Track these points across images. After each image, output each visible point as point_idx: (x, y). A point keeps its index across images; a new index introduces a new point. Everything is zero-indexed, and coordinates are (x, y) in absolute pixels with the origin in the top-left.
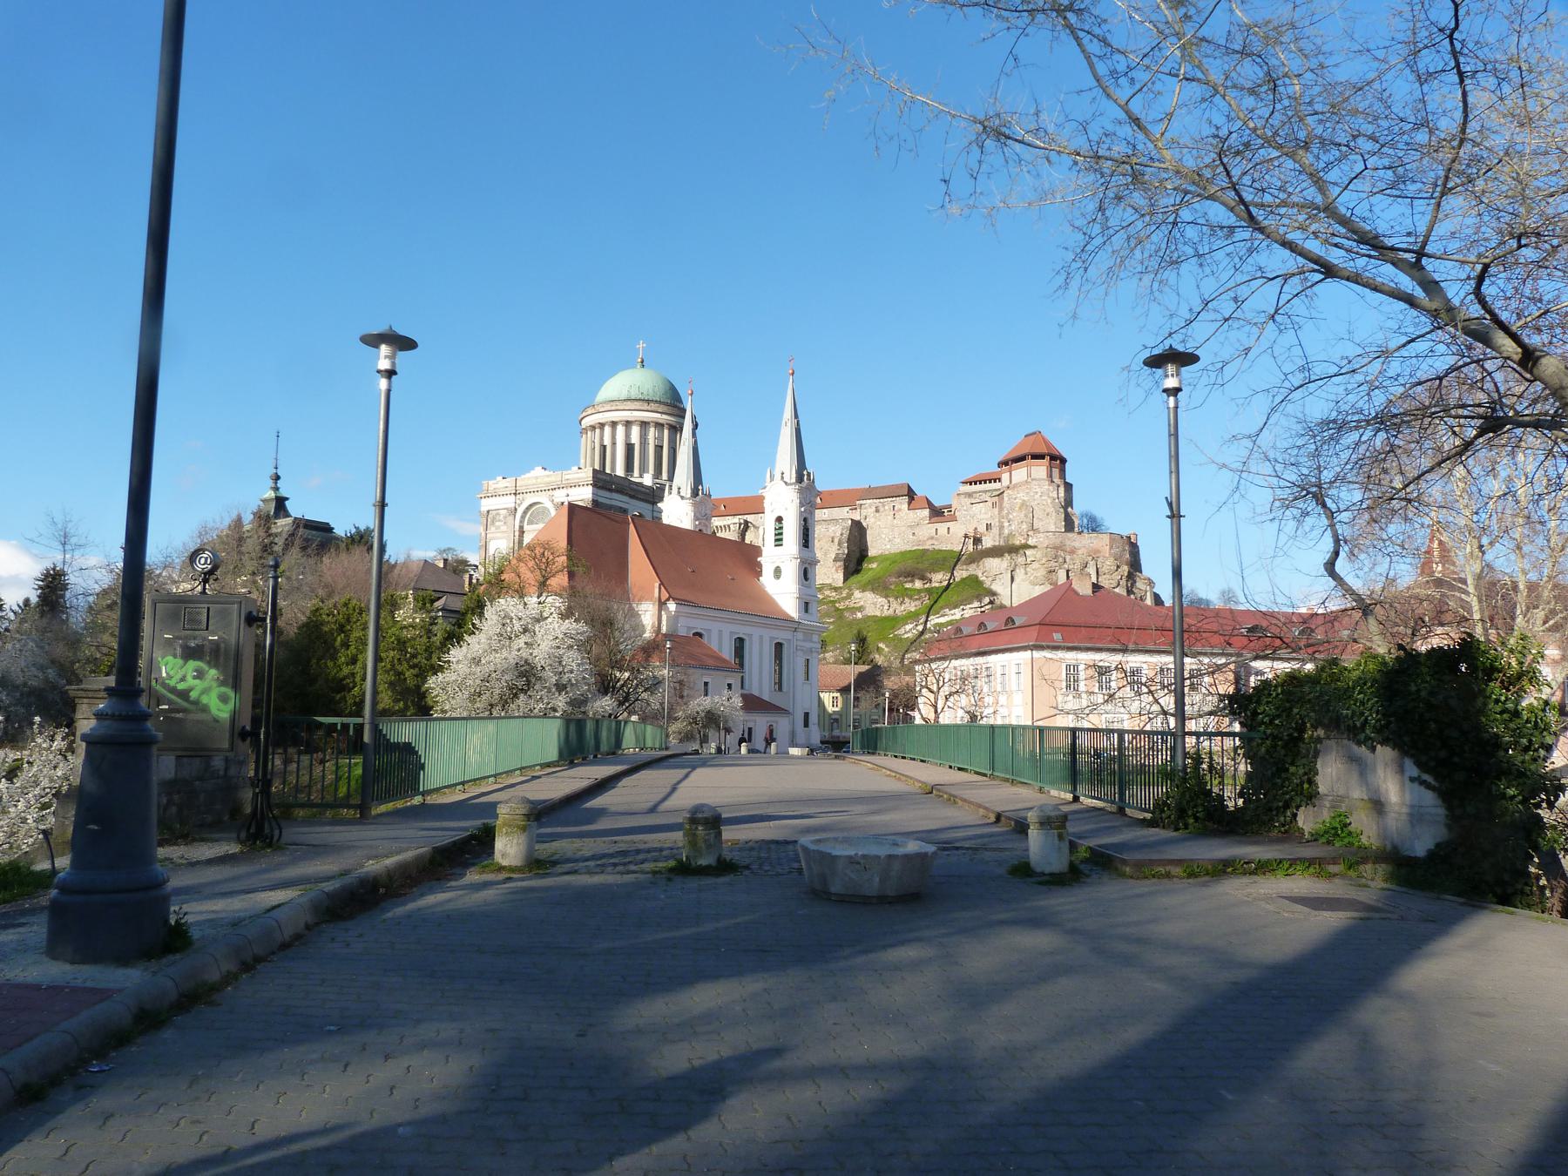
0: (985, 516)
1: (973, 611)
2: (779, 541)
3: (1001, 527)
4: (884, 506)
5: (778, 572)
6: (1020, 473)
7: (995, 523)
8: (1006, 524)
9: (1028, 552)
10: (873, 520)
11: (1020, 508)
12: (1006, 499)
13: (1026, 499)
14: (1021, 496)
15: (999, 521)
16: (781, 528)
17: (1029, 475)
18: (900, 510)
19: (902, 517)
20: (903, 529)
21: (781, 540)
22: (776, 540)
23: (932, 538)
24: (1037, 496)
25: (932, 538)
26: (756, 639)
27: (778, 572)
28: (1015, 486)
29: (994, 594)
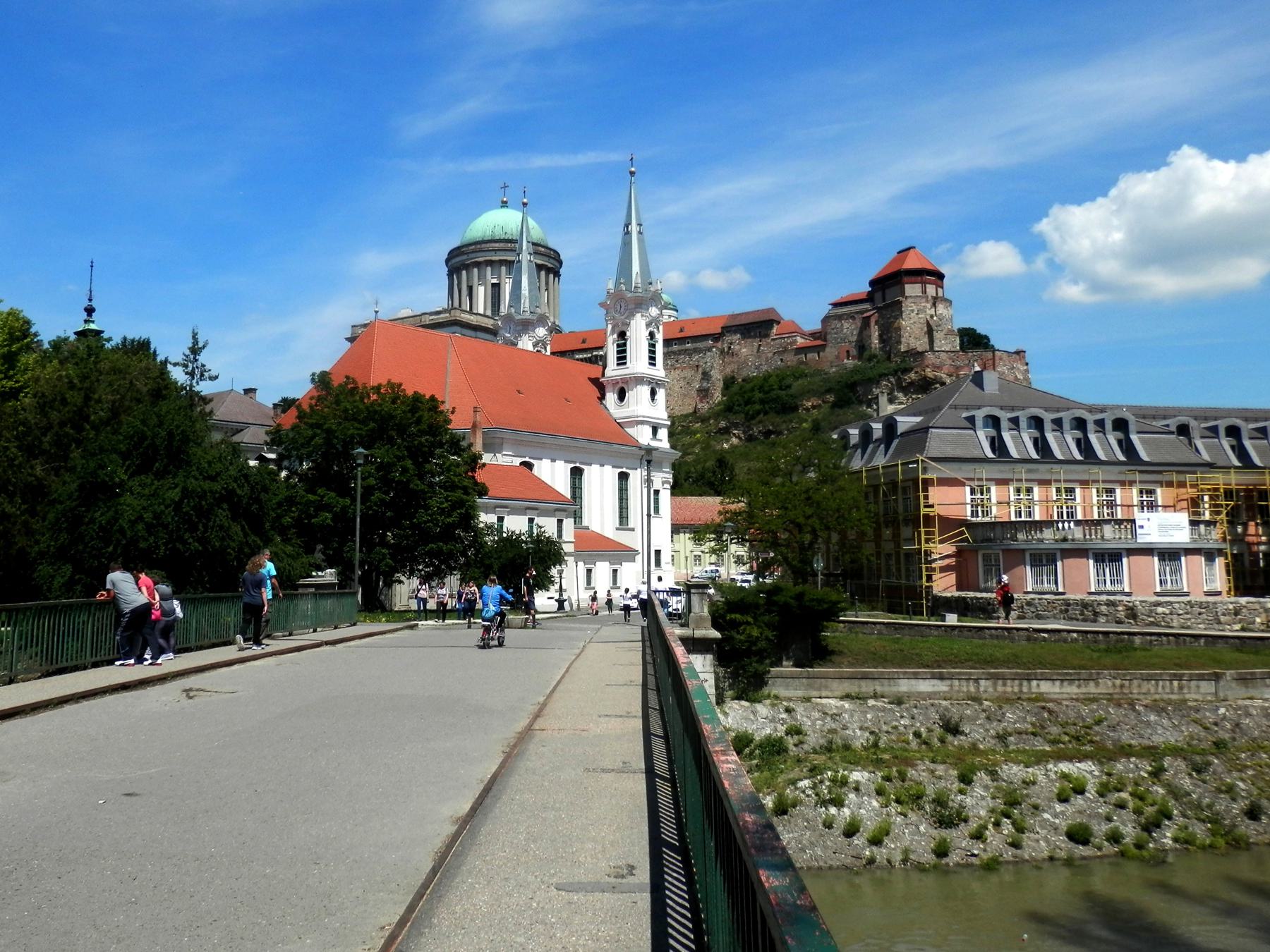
2: (622, 360)
10: (737, 347)
16: (625, 345)
19: (769, 343)
21: (625, 358)
22: (619, 359)
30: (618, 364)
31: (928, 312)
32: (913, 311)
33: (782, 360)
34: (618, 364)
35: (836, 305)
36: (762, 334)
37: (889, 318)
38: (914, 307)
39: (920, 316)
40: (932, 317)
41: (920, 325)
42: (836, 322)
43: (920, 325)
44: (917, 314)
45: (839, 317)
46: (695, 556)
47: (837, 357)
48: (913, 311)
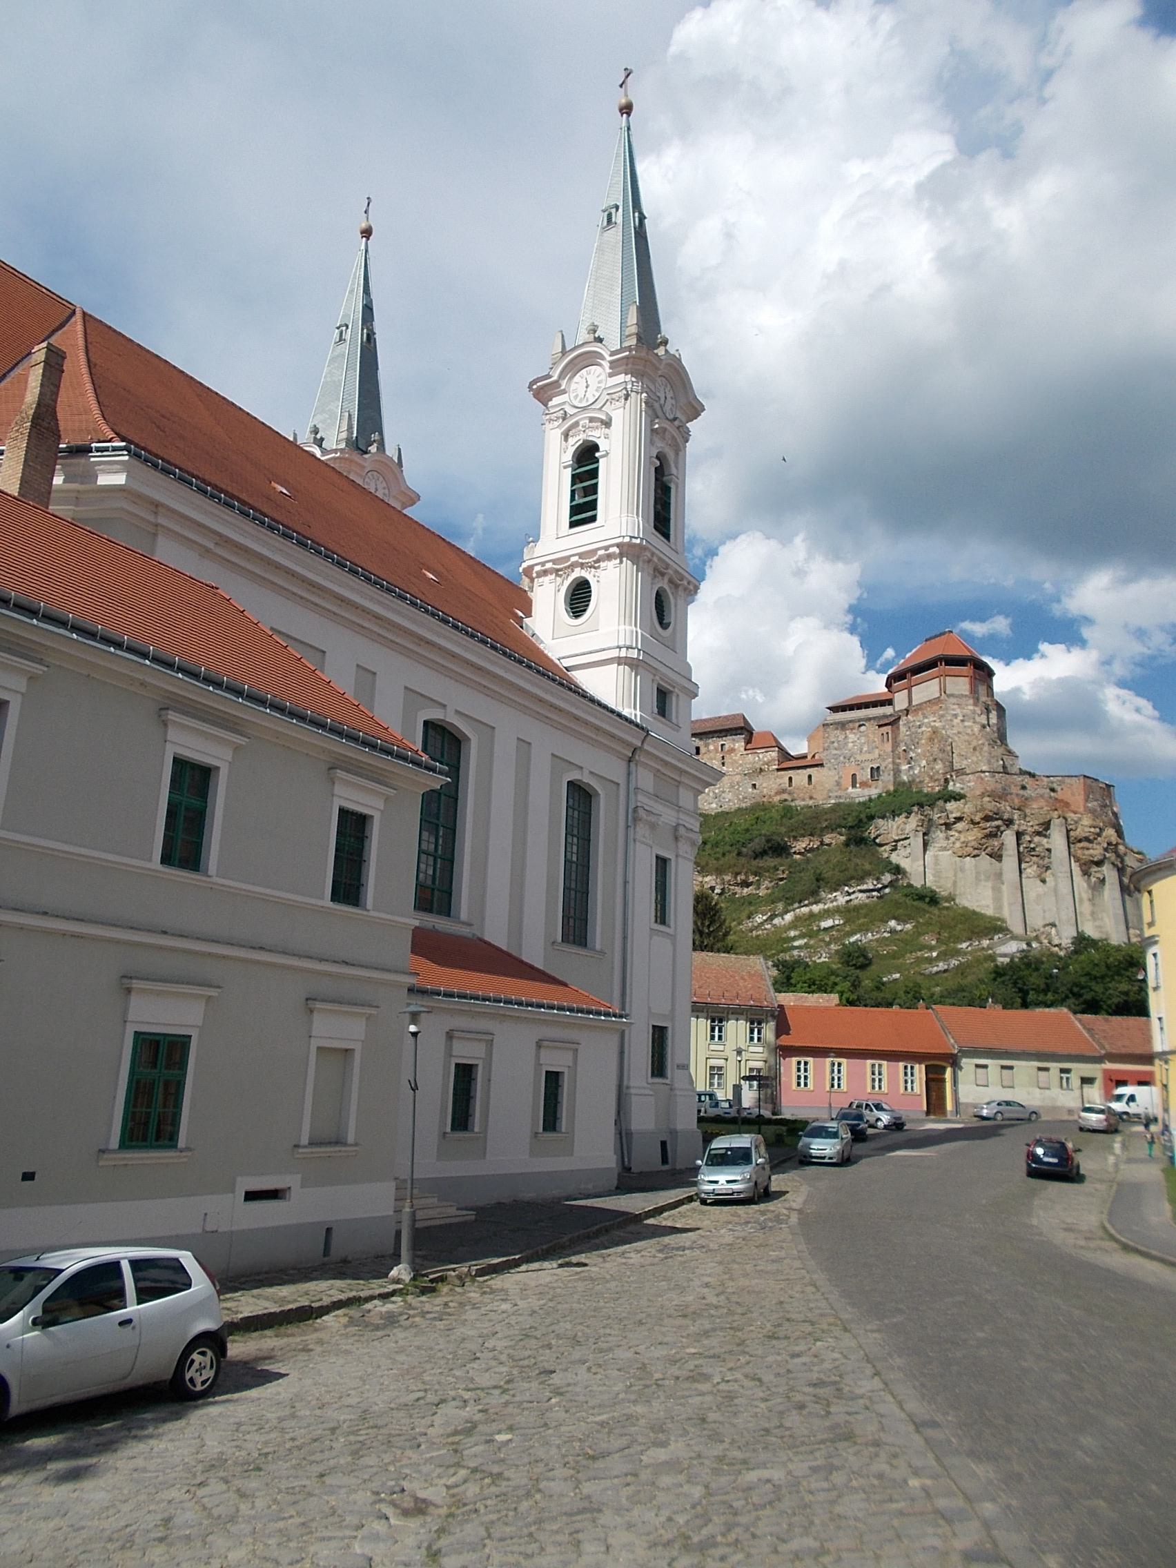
0: (870, 757)
1: (860, 895)
3: (897, 772)
4: (707, 745)
5: (579, 598)
6: (926, 689)
7: (887, 764)
8: (905, 767)
9: (951, 806)
11: (931, 739)
12: (903, 729)
13: (937, 724)
14: (931, 720)
15: (894, 763)
17: (943, 690)
18: (732, 750)
19: (736, 761)
20: (738, 778)
21: (592, 505)
22: (575, 510)
23: (784, 791)
24: (956, 721)
25: (784, 791)
26: (505, 747)
27: (579, 598)
28: (920, 707)
29: (897, 870)
30: (573, 524)
31: (978, 719)
32: (956, 716)
33: (754, 786)
34: (573, 524)
35: (834, 709)
36: (727, 747)
37: (920, 727)
38: (958, 711)
39: (966, 724)
40: (984, 727)
41: (967, 738)
42: (838, 732)
43: (967, 738)
44: (962, 721)
45: (842, 725)
46: (712, 1068)
47: (838, 784)
48: (956, 716)
